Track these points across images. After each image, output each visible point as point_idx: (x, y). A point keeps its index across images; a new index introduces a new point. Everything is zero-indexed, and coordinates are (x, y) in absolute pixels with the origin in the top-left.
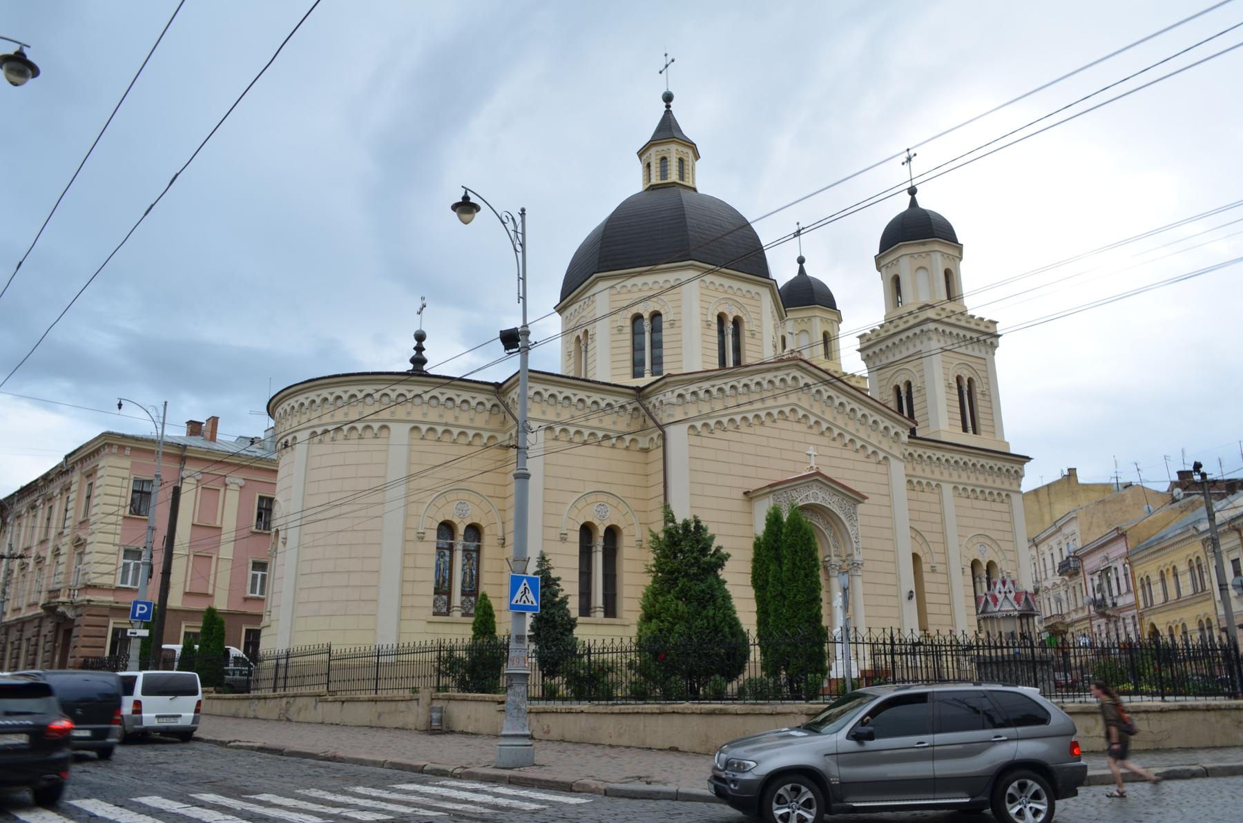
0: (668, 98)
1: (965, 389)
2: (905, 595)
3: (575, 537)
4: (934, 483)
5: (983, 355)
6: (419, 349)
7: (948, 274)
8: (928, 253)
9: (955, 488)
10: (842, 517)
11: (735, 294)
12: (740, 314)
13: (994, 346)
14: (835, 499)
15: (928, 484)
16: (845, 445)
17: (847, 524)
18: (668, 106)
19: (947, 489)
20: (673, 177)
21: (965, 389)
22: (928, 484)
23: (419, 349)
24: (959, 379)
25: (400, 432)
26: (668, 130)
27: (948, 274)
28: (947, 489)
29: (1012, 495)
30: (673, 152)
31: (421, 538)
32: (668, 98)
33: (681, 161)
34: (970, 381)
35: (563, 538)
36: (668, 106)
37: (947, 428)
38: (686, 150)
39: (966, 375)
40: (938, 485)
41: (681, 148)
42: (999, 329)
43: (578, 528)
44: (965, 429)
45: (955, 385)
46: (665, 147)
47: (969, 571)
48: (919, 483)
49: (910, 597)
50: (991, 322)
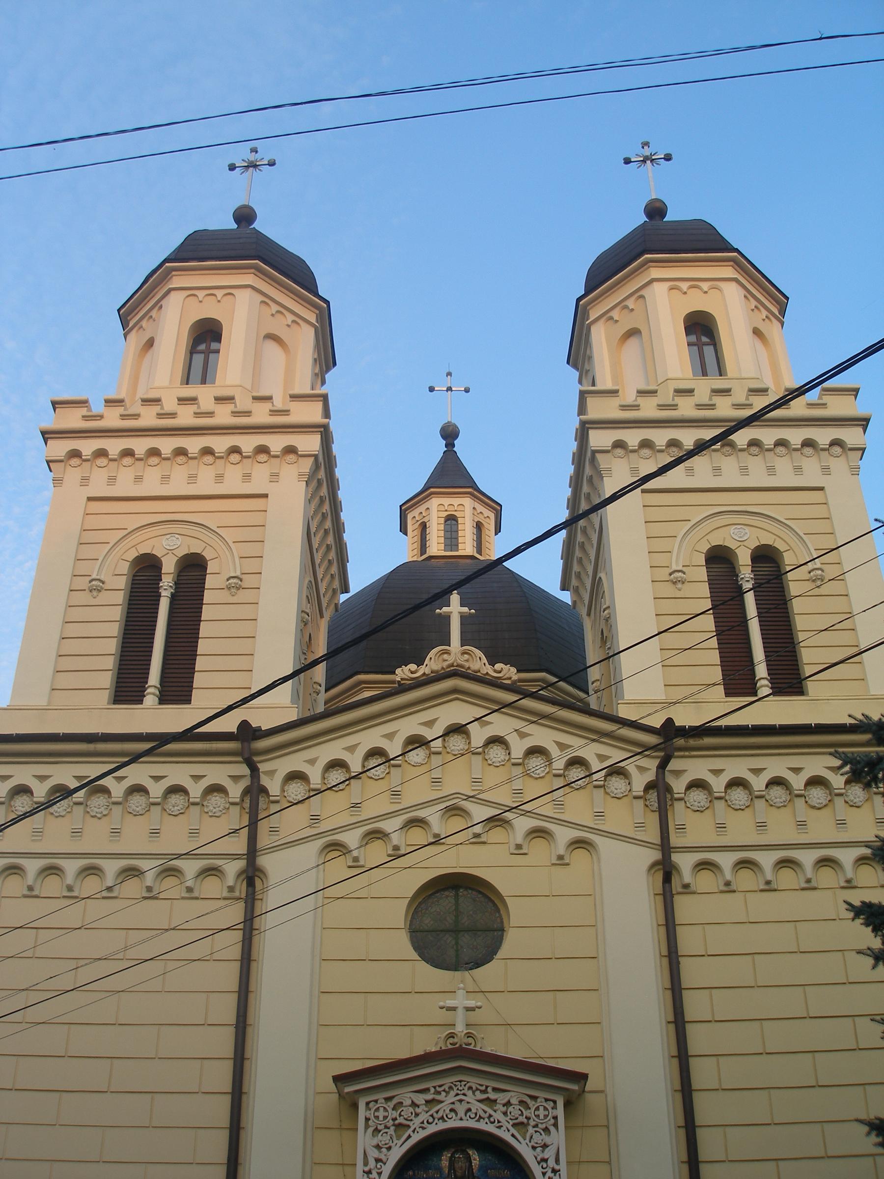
5: (811, 474)
7: (701, 328)
8: (638, 294)
24: (719, 559)
27: (701, 328)
34: (766, 558)
37: (659, 694)
45: (702, 574)
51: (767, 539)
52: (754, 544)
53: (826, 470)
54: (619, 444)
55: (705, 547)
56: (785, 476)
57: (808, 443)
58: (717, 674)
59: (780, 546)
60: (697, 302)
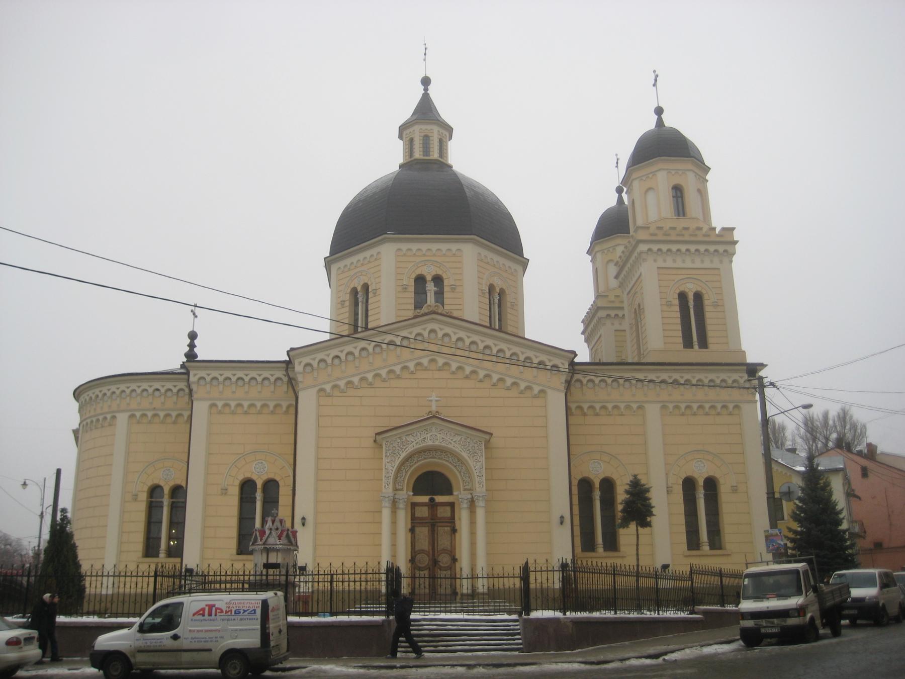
0: (426, 82)
1: (691, 304)
2: (556, 519)
3: (235, 491)
4: (635, 406)
6: (192, 346)
7: (678, 191)
8: (654, 173)
9: (664, 407)
10: (465, 455)
11: (434, 255)
12: (440, 273)
13: (730, 254)
14: (458, 438)
15: (628, 407)
16: (494, 385)
17: (471, 462)
18: (426, 90)
19: (653, 411)
20: (418, 155)
21: (691, 304)
22: (628, 407)
23: (192, 346)
24: (682, 296)
25: (122, 419)
26: (426, 111)
27: (678, 191)
28: (653, 411)
29: (741, 405)
30: (417, 132)
31: (135, 498)
32: (426, 82)
33: (426, 139)
34: (698, 297)
35: (224, 492)
36: (426, 90)
38: (429, 127)
39: (690, 289)
40: (640, 407)
41: (424, 127)
42: (736, 236)
43: (237, 483)
44: (688, 344)
45: (677, 302)
46: (411, 130)
47: (679, 489)
48: (616, 407)
49: (562, 523)
50: (724, 229)
51: (699, 289)
52: (694, 290)
53: (721, 262)
54: (650, 250)
55: (678, 291)
56: (707, 264)
57: (716, 251)
58: (680, 340)
59: (704, 292)
60: (677, 180)
